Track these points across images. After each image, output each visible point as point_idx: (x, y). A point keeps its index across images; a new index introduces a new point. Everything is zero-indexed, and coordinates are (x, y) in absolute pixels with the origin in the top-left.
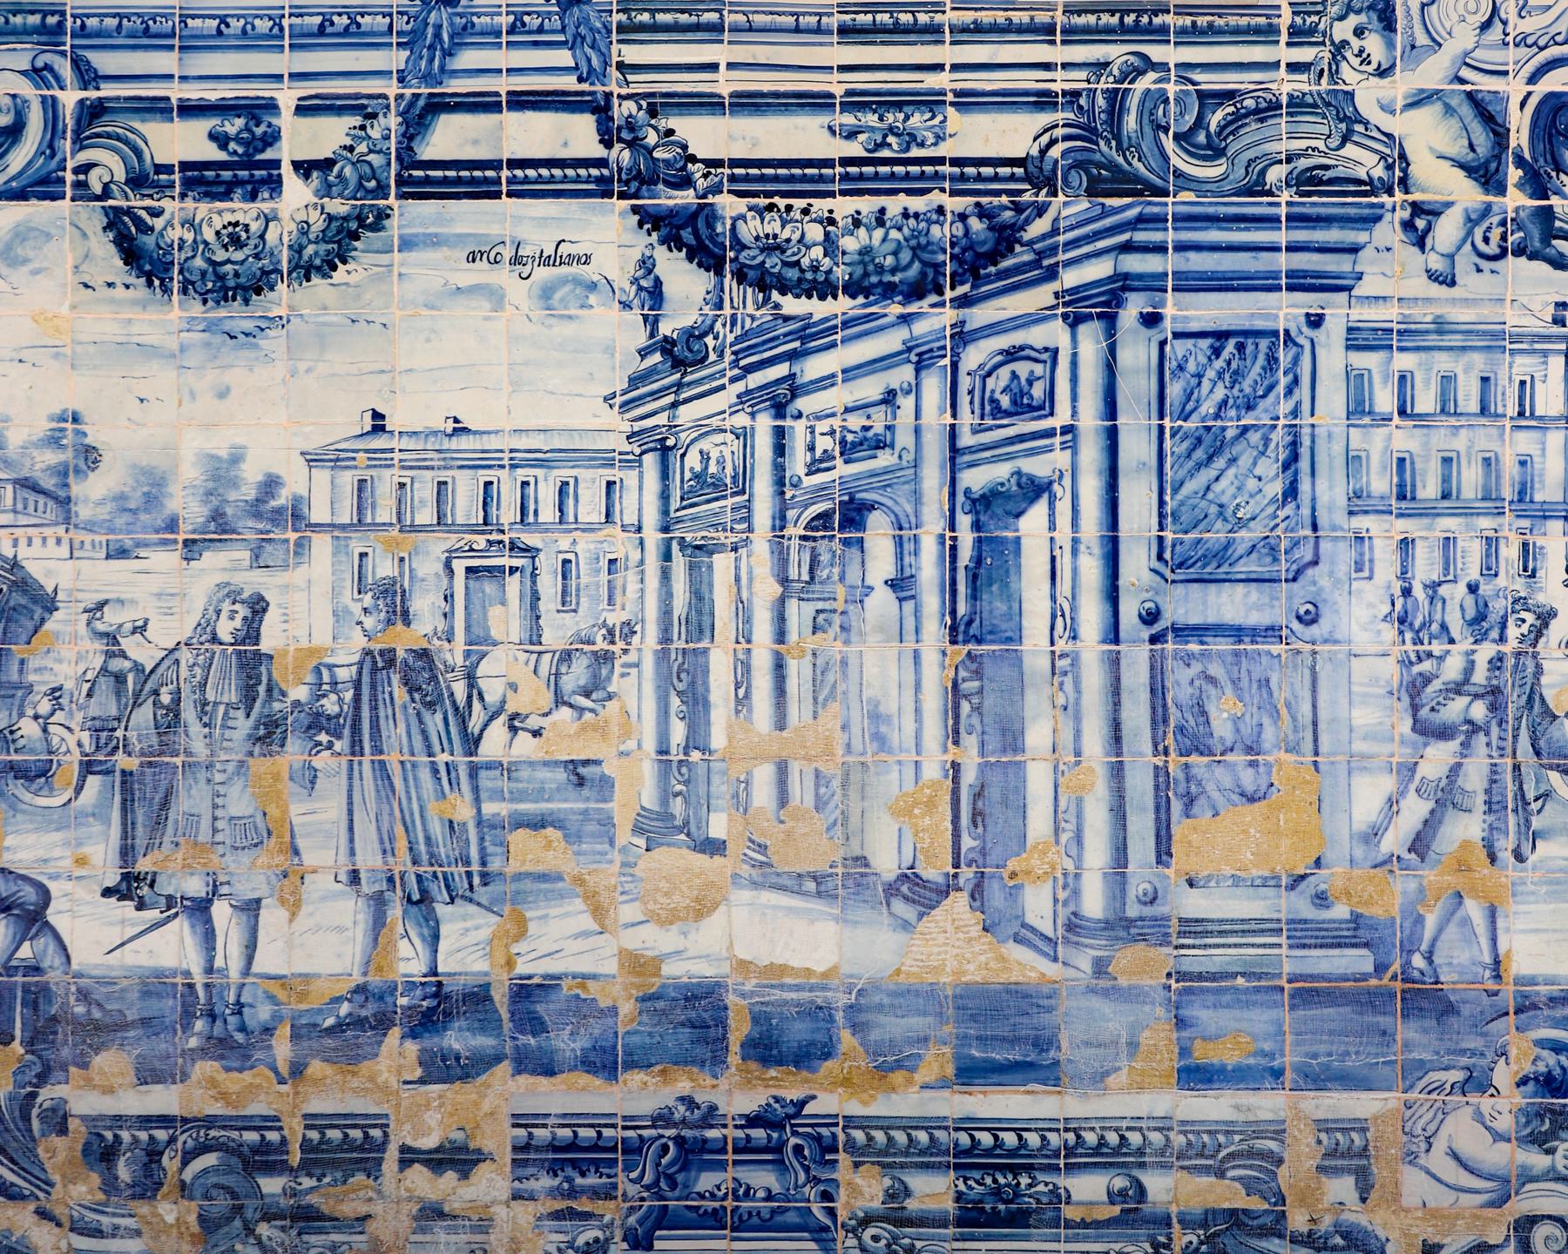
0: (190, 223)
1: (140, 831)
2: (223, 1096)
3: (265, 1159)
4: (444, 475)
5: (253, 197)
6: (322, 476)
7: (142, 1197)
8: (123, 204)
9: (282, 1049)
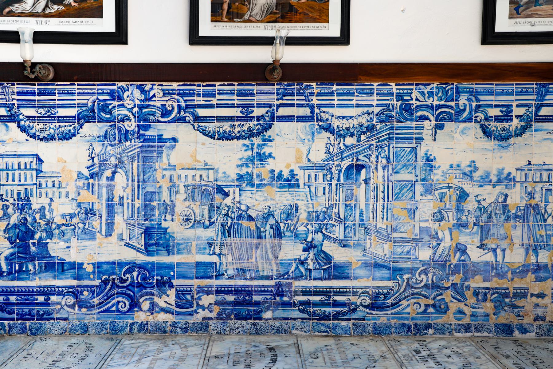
0: (495, 127)
1: (484, 236)
2: (498, 284)
3: (506, 295)
4: (541, 172)
5: (507, 122)
6: (519, 172)
7: (483, 302)
8: (484, 123)
9: (509, 275)
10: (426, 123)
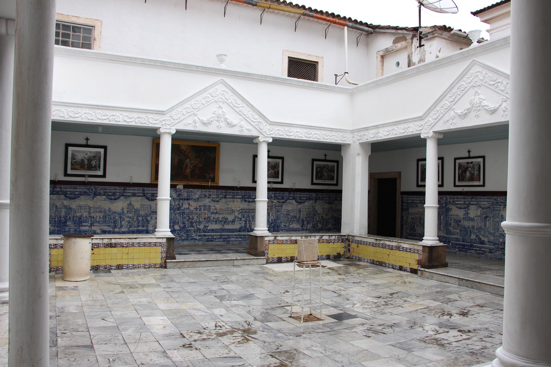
10: (501, 206)
